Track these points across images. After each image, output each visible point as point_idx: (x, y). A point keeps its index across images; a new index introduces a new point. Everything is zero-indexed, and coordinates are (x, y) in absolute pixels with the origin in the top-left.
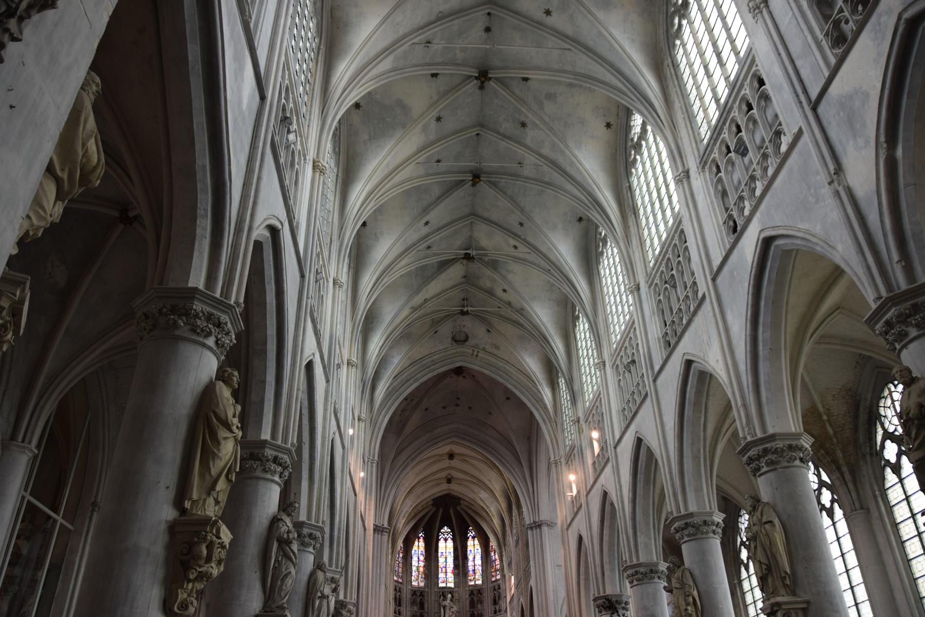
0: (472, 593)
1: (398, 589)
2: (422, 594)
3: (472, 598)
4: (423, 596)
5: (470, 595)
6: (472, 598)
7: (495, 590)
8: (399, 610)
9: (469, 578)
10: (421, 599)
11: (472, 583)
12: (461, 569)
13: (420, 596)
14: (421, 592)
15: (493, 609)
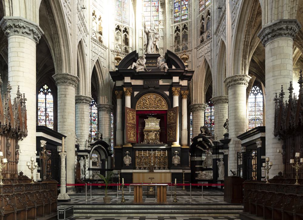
0: (177, 29)
1: (98, 17)
2: (125, 31)
3: (177, 34)
4: (127, 32)
5: (176, 31)
6: (177, 34)
7: (203, 19)
8: (100, 38)
9: (175, 15)
10: (125, 35)
11: (178, 19)
12: (167, 5)
13: (124, 31)
14: (126, 29)
15: (200, 39)
